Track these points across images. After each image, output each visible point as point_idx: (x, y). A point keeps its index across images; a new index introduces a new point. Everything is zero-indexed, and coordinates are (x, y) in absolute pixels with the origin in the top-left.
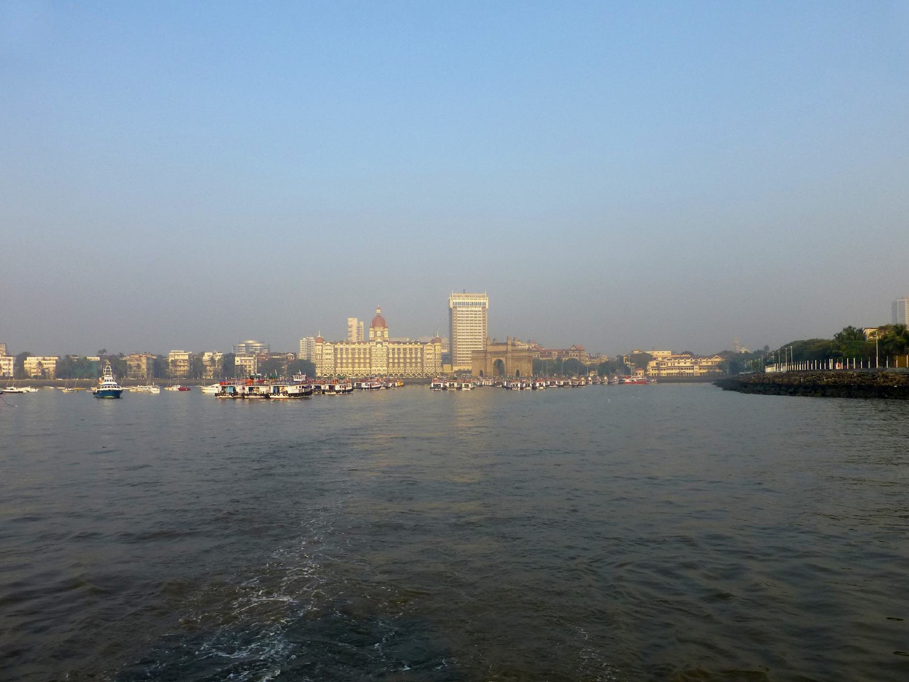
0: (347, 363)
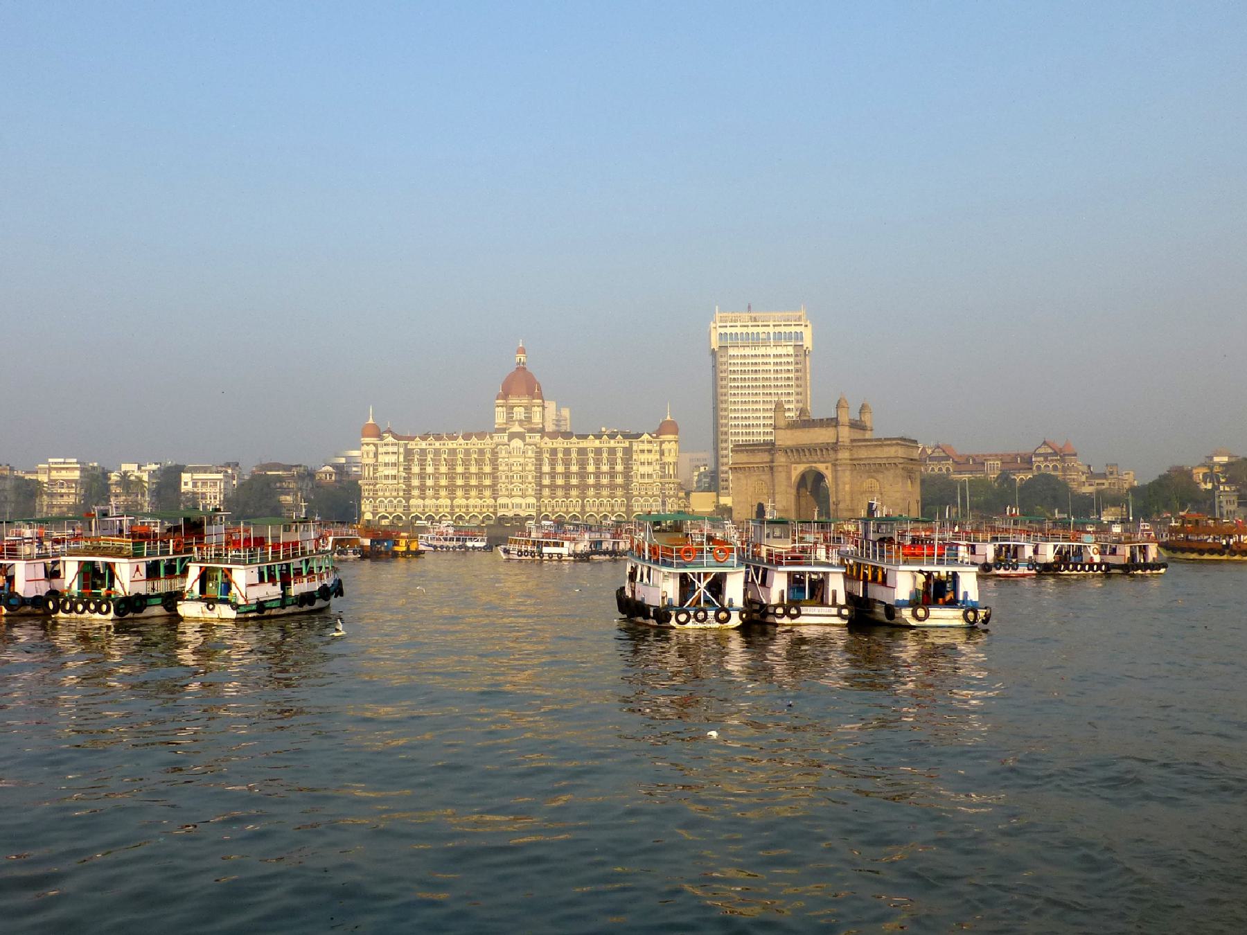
0: (436, 488)
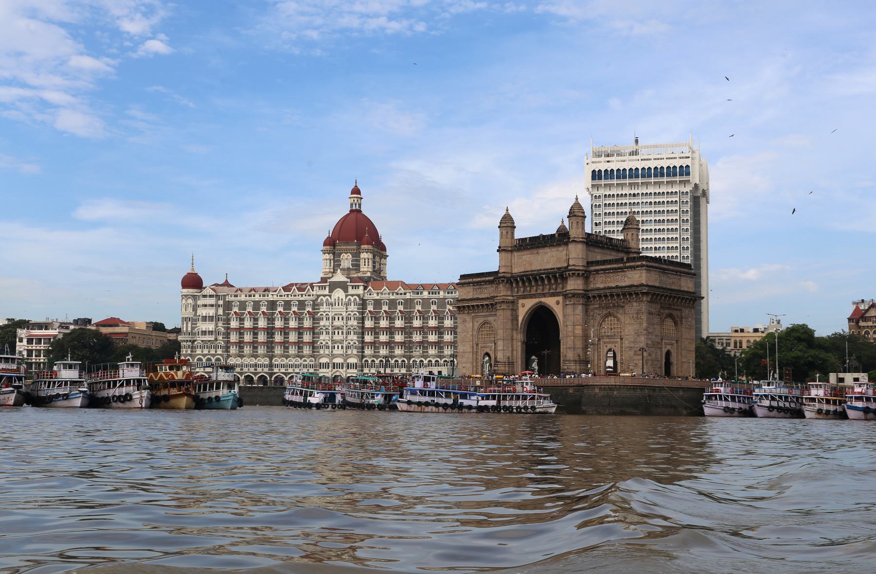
0: (254, 345)
